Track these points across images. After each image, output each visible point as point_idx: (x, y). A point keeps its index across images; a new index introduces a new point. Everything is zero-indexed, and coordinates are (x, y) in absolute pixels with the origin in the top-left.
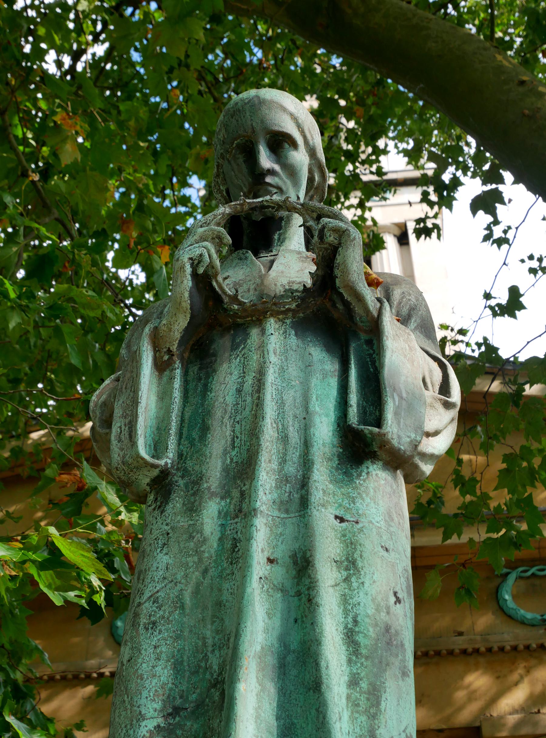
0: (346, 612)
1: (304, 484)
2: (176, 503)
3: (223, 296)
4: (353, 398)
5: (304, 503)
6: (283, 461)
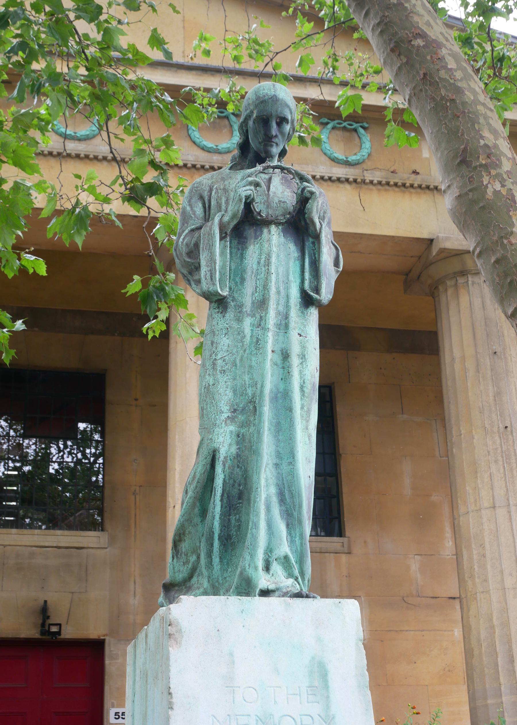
0: (301, 378)
1: (286, 317)
2: (230, 314)
3: (254, 212)
4: (307, 275)
5: (287, 326)
6: (278, 304)
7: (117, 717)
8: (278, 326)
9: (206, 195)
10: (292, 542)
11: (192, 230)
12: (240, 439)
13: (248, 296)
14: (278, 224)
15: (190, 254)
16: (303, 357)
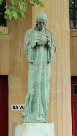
1: (44, 66)
2: (33, 66)
4: (48, 57)
5: (44, 68)
7: (14, 108)
8: (42, 68)
9: (29, 36)
10: (44, 111)
11: (26, 45)
12: (35, 91)
13: (36, 62)
14: (43, 46)
15: (26, 51)
16: (47, 74)
